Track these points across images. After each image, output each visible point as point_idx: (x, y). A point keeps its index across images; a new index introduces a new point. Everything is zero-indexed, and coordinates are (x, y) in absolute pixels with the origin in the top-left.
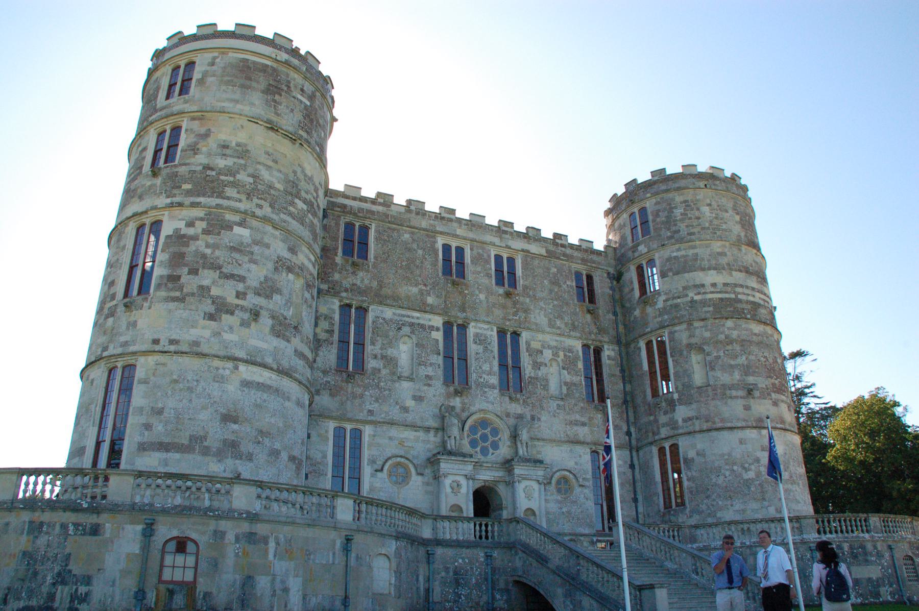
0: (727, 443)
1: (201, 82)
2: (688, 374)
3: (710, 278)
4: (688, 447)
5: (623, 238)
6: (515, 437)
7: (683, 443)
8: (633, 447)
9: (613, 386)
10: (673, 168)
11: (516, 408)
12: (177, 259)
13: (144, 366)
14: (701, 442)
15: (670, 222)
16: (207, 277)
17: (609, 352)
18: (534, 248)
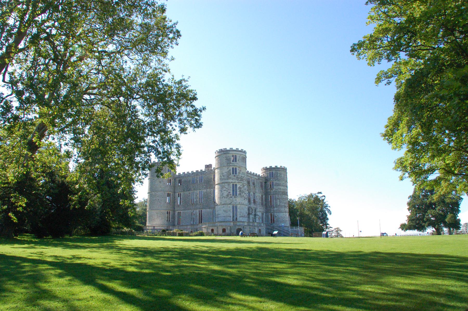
0: (281, 214)
1: (238, 160)
2: (277, 203)
3: (282, 188)
4: (276, 214)
5: (267, 176)
6: (255, 211)
7: (275, 213)
8: (266, 213)
9: (264, 203)
10: (279, 167)
11: (255, 206)
12: (240, 191)
13: (238, 206)
14: (278, 214)
15: (277, 176)
16: (243, 194)
17: (264, 196)
18: (257, 178)
